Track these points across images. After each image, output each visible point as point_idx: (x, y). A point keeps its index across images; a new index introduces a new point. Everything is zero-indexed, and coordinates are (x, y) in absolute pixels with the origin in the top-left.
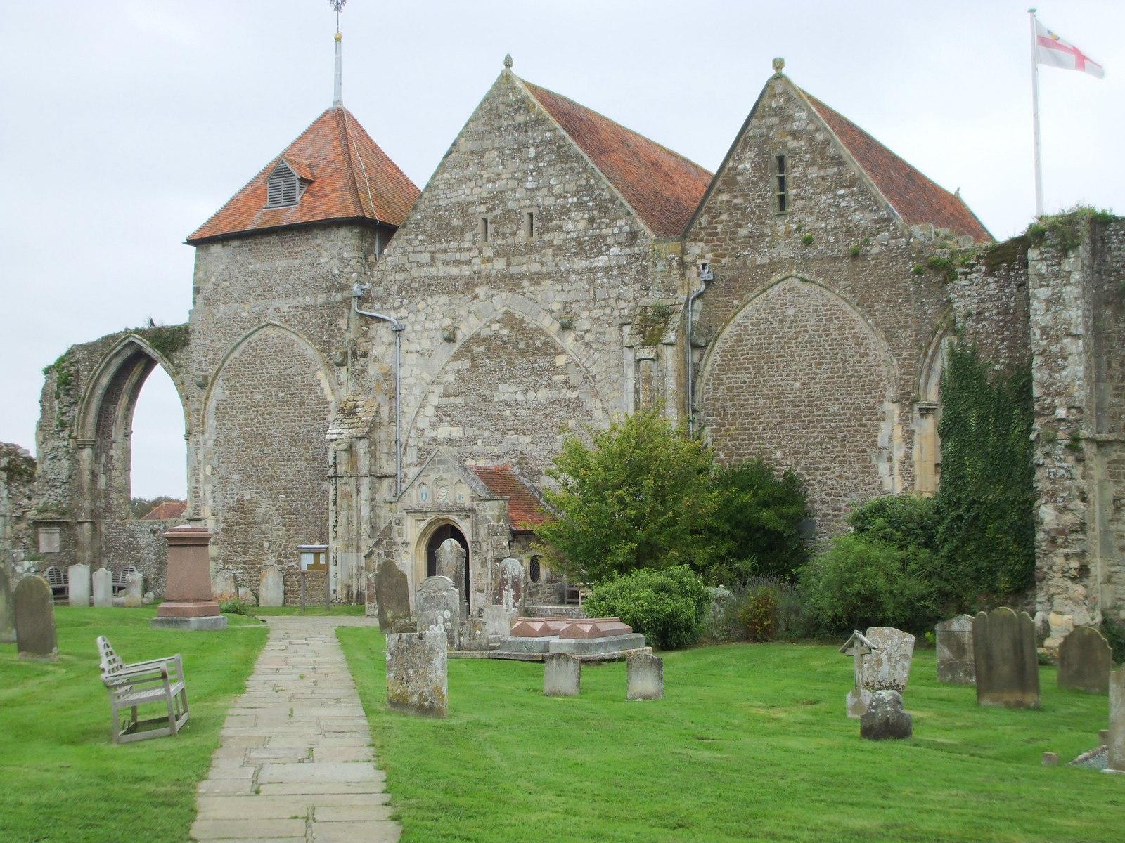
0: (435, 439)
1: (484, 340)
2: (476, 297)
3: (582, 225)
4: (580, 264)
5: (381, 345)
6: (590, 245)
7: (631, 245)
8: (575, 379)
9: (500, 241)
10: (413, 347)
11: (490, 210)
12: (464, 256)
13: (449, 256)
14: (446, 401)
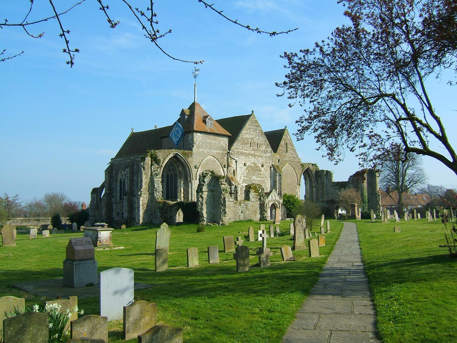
0: (243, 186)
1: (251, 167)
2: (249, 158)
3: (265, 148)
4: (265, 155)
5: (233, 165)
6: (266, 152)
7: (271, 153)
8: (264, 177)
9: (253, 148)
10: (239, 166)
11: (251, 141)
12: (247, 149)
13: (245, 148)
14: (244, 178)
